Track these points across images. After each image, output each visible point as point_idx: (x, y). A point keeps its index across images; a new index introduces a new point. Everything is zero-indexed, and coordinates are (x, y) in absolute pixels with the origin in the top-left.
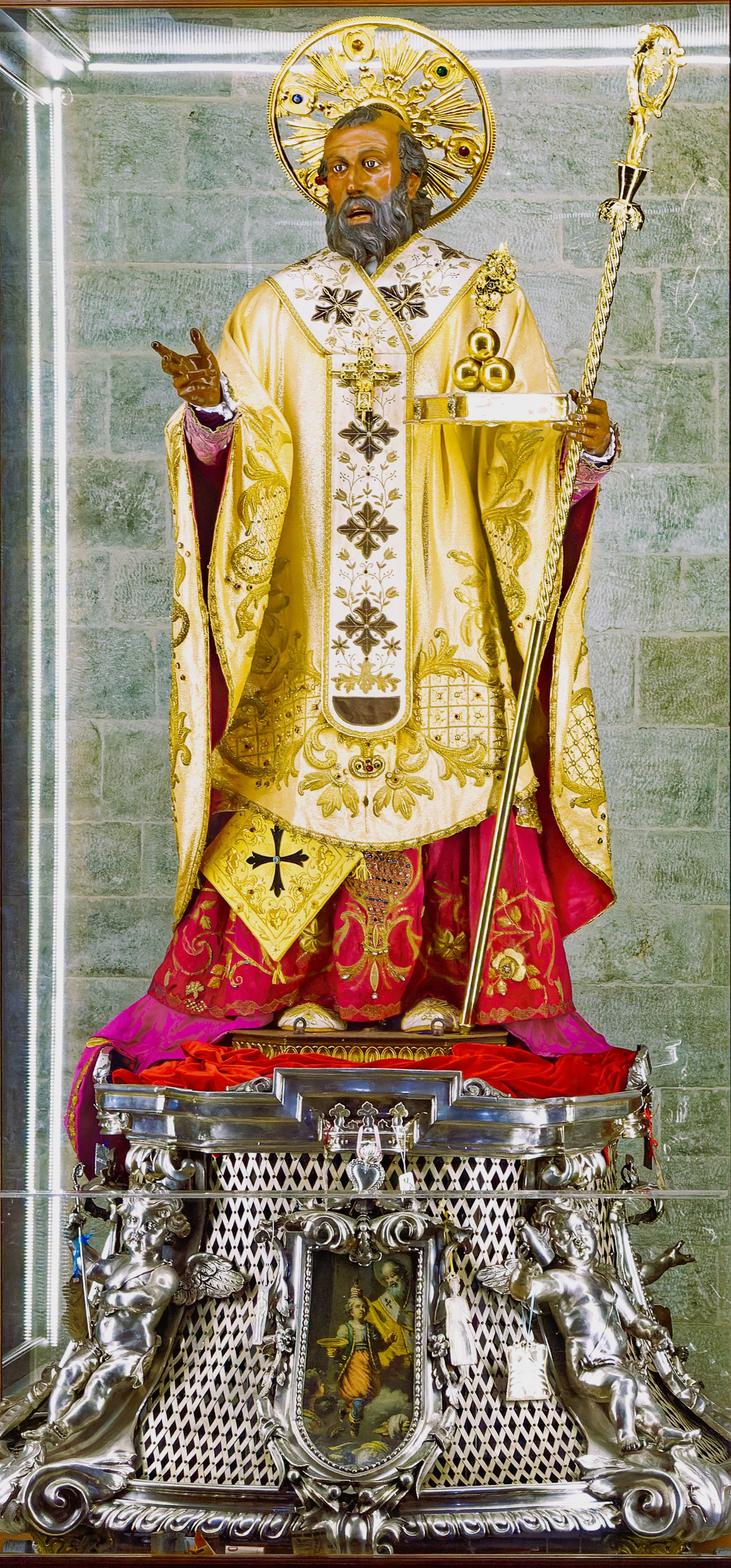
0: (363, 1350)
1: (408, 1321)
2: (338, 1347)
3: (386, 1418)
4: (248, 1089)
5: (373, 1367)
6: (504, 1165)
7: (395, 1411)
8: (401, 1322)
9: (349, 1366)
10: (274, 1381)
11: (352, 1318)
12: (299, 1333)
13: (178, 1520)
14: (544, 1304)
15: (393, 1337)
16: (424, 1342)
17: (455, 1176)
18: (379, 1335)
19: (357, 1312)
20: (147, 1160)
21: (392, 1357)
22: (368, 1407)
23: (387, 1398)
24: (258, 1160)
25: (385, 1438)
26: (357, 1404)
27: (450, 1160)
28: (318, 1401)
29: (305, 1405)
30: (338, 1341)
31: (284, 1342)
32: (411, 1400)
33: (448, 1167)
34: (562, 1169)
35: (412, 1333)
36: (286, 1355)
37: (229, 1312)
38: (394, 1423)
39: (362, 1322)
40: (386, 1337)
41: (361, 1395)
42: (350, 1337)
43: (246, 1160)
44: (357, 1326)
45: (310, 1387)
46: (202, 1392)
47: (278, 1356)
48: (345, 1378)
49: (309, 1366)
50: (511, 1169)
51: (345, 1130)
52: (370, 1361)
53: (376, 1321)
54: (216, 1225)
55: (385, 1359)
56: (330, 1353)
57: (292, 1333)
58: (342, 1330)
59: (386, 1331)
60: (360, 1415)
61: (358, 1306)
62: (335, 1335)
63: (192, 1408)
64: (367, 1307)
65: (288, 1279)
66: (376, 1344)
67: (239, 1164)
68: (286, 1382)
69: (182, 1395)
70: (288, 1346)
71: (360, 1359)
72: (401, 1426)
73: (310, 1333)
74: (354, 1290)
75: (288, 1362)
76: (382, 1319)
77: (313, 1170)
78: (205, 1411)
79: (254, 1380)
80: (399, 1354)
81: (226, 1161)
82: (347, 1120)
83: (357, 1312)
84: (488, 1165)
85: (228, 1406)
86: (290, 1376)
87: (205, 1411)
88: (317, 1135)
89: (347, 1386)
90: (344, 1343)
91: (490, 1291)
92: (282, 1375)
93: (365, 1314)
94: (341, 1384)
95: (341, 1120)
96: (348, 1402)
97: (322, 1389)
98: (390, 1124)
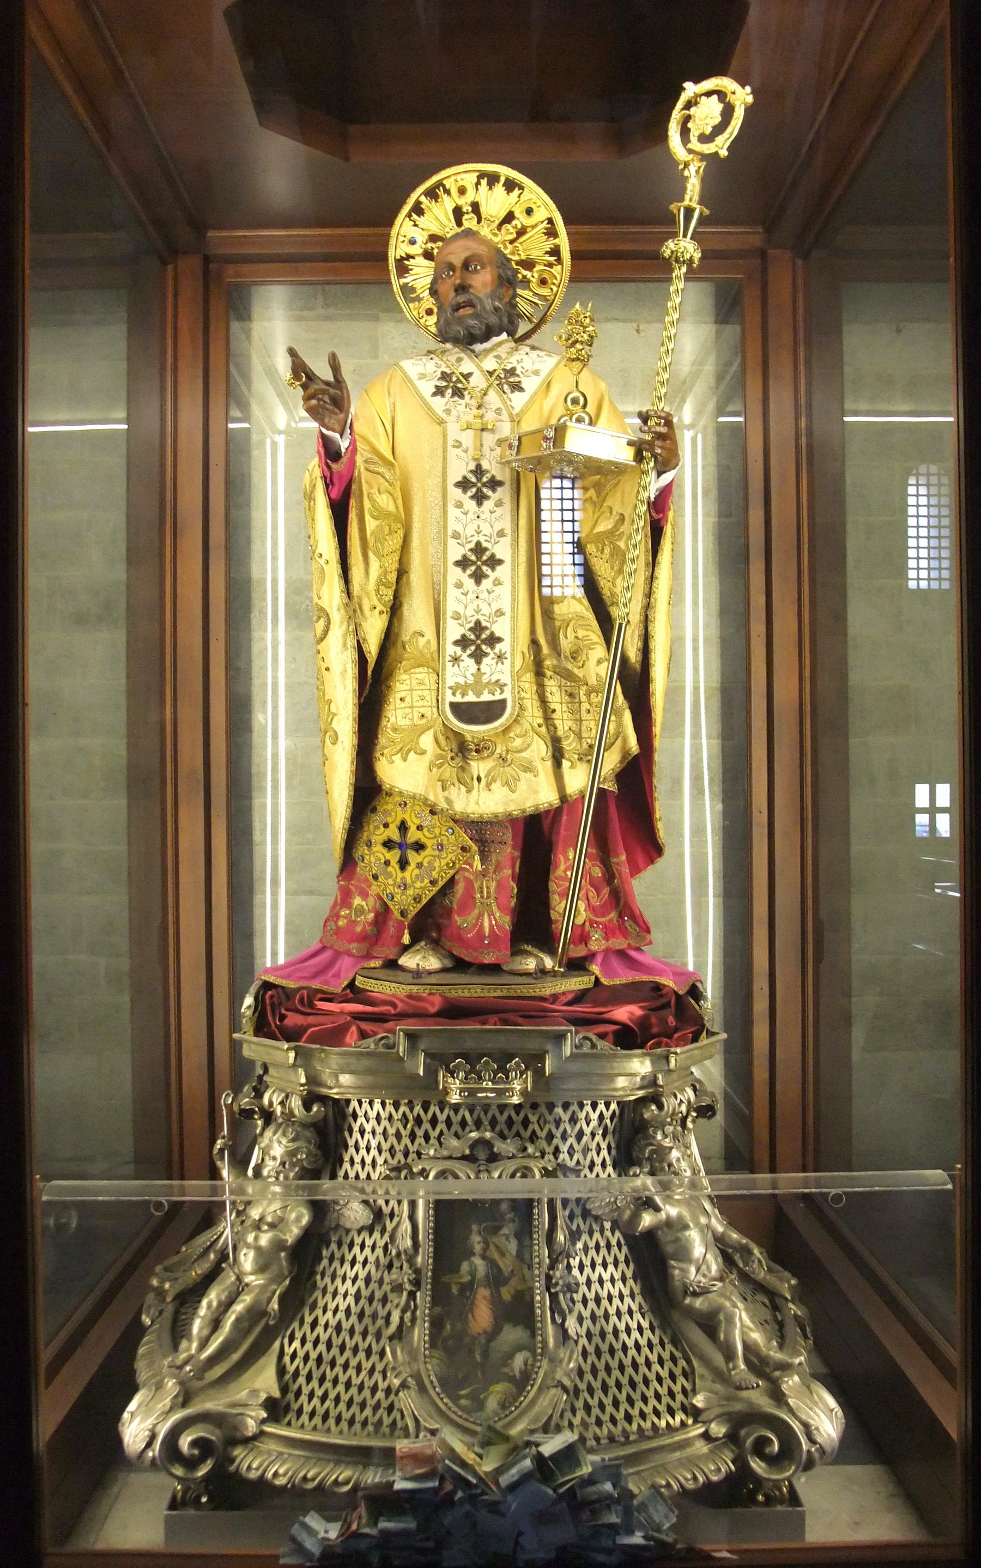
0: (485, 1287)
1: (527, 1256)
2: (462, 1284)
3: (511, 1356)
4: (372, 1046)
5: (496, 1301)
6: (607, 1105)
7: (520, 1348)
8: (520, 1255)
9: (473, 1303)
10: (402, 1318)
11: (474, 1254)
12: (424, 1271)
13: (309, 1476)
14: (650, 1234)
15: (512, 1271)
16: (543, 1277)
17: (565, 1117)
18: (499, 1269)
19: (478, 1248)
20: (282, 1103)
21: (513, 1292)
22: (493, 1344)
23: (512, 1334)
24: (383, 1104)
25: (511, 1379)
26: (483, 1341)
27: (560, 1104)
28: (445, 1340)
29: (433, 1343)
30: (461, 1277)
31: (410, 1281)
32: (533, 1335)
33: (559, 1110)
34: (660, 1107)
35: (530, 1267)
36: (412, 1295)
37: (358, 1241)
38: (519, 1360)
39: (484, 1257)
40: (506, 1270)
41: (485, 1332)
42: (473, 1273)
43: (371, 1103)
44: (479, 1262)
45: (436, 1324)
46: (333, 1322)
47: (405, 1294)
48: (470, 1315)
49: (435, 1301)
50: (613, 1106)
51: (465, 1083)
52: (492, 1294)
53: (496, 1256)
54: (347, 1158)
55: (506, 1294)
56: (455, 1290)
57: (417, 1271)
58: (465, 1267)
59: (506, 1265)
60: (486, 1354)
61: (479, 1243)
62: (458, 1271)
63: (324, 1337)
64: (486, 1243)
65: (412, 1217)
66: (496, 1279)
67: (366, 1105)
68: (413, 1320)
69: (314, 1324)
70: (414, 1285)
71: (483, 1293)
72: (526, 1364)
73: (434, 1271)
74: (475, 1227)
75: (415, 1299)
76: (503, 1255)
77: (434, 1115)
78: (336, 1342)
79: (382, 1313)
80: (520, 1287)
81: (354, 1104)
82: (467, 1074)
83: (478, 1248)
84: (594, 1106)
85: (357, 1338)
86: (418, 1312)
87: (336, 1342)
88: (437, 1083)
89: (472, 1324)
90: (466, 1279)
91: (597, 1218)
92: (408, 1314)
93: (486, 1249)
94: (465, 1322)
95: (462, 1075)
96: (474, 1339)
97: (448, 1327)
98: (507, 1078)
